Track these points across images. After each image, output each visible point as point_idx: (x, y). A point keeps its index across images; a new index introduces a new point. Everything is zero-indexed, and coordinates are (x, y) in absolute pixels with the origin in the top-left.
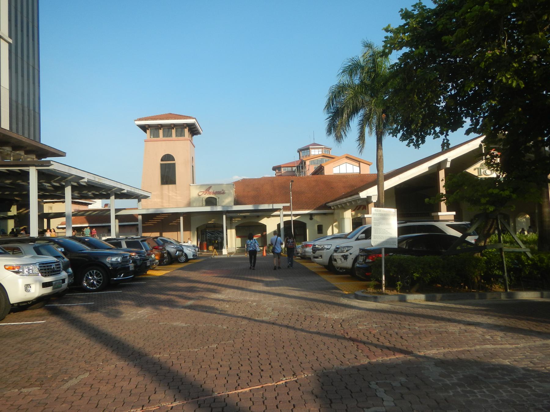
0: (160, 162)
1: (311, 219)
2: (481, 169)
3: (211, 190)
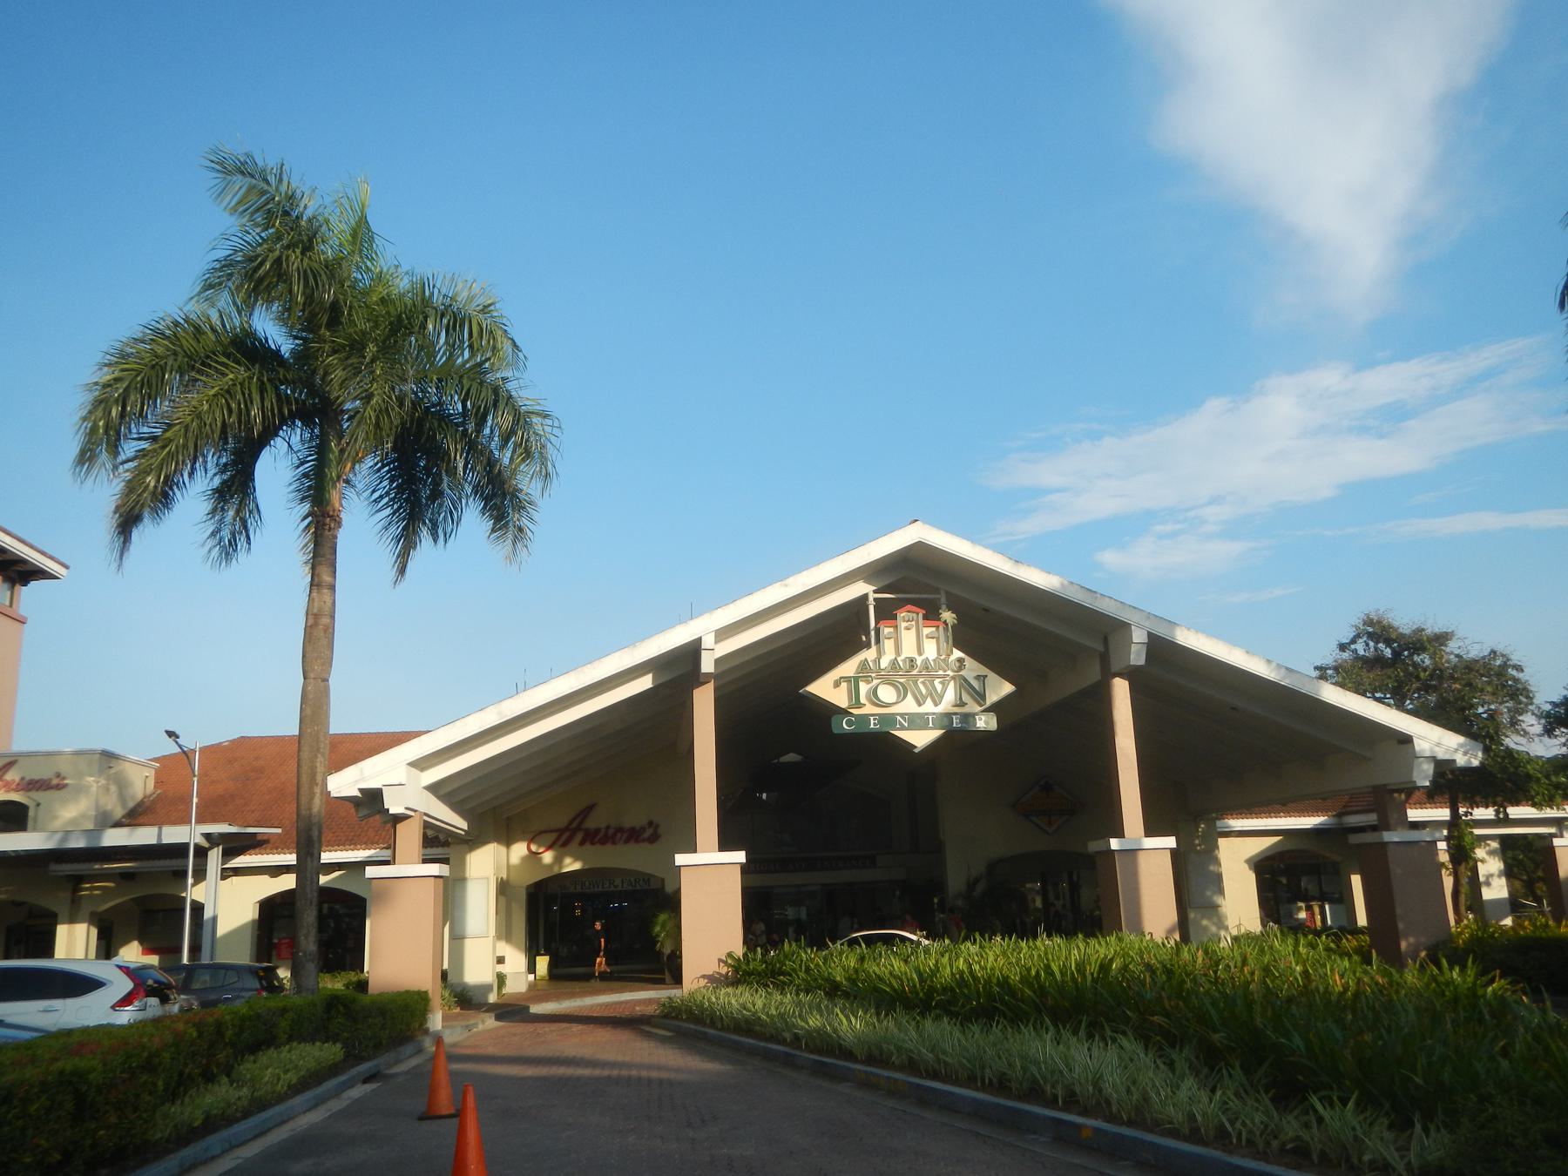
2: (857, 680)
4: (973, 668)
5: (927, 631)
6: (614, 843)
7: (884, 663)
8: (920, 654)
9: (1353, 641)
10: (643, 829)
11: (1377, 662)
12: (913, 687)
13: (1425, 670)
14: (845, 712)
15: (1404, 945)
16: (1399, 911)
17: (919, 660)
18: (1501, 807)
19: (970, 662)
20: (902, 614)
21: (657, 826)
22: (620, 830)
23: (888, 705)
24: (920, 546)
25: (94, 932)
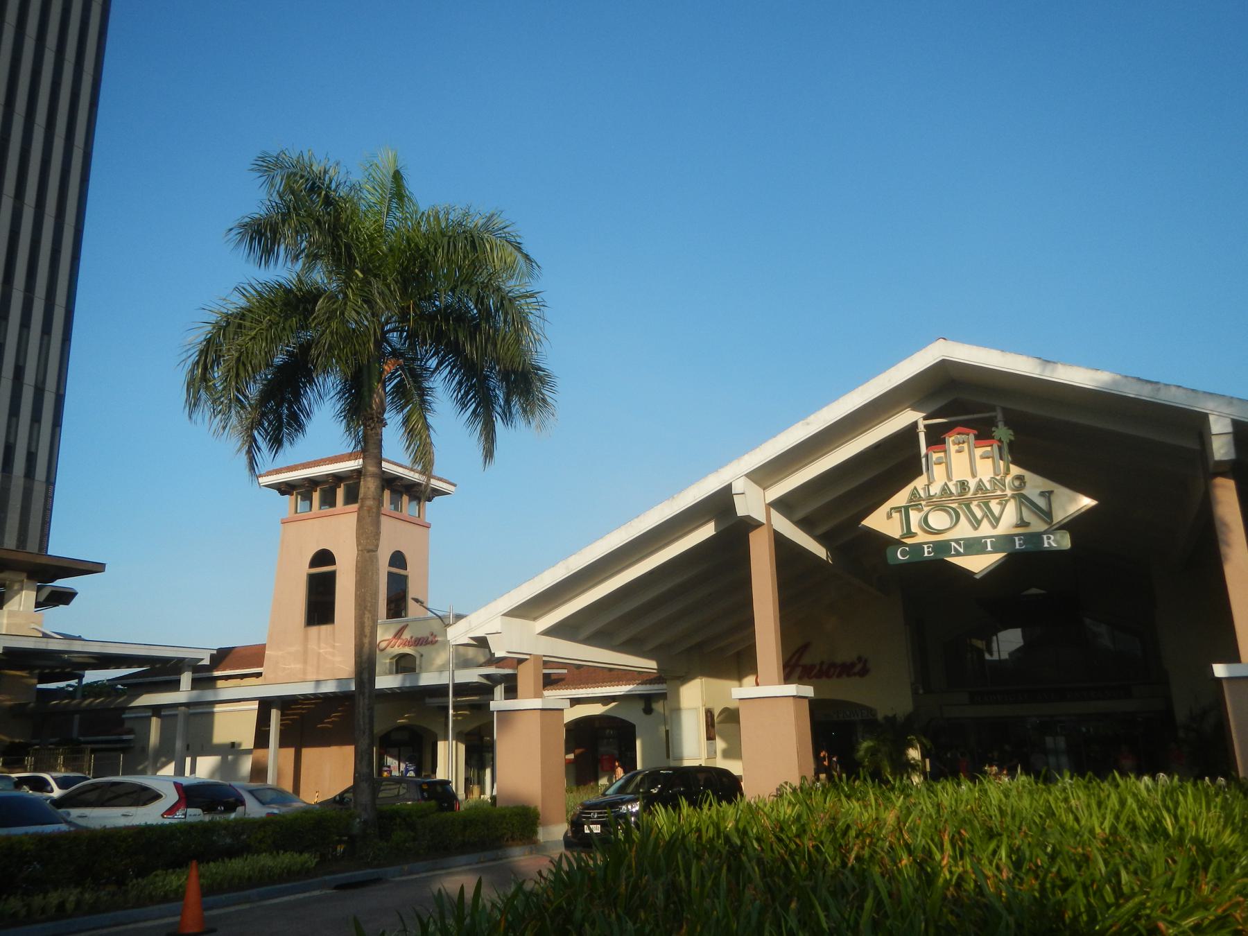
0: (302, 570)
1: (648, 710)
3: (406, 635)
4: (1035, 484)
5: (979, 452)
6: (829, 677)
7: (935, 489)
8: (974, 476)
10: (853, 665)
12: (969, 509)
14: (898, 543)
17: (972, 484)
19: (1028, 475)
20: (951, 440)
21: (866, 661)
22: (833, 665)
23: (939, 532)
24: (944, 367)
25: (462, 747)
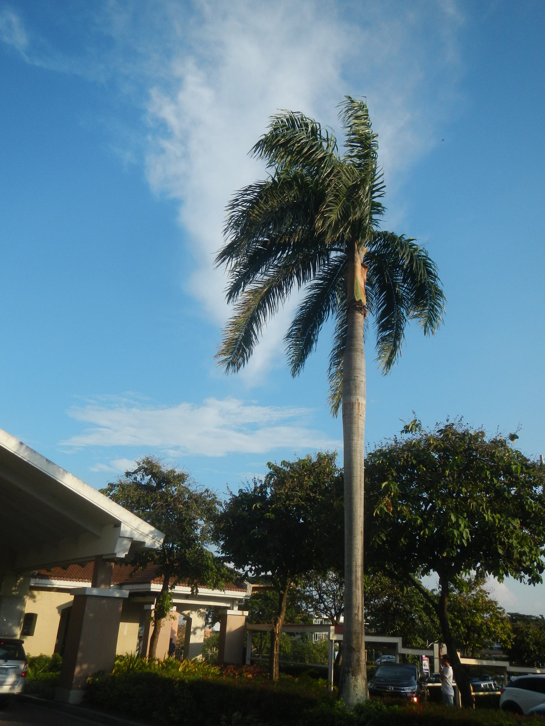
9: (135, 472)
11: (148, 487)
13: (172, 497)
15: (77, 669)
16: (81, 643)
18: (194, 586)
